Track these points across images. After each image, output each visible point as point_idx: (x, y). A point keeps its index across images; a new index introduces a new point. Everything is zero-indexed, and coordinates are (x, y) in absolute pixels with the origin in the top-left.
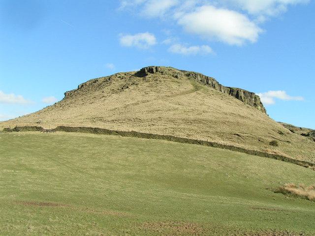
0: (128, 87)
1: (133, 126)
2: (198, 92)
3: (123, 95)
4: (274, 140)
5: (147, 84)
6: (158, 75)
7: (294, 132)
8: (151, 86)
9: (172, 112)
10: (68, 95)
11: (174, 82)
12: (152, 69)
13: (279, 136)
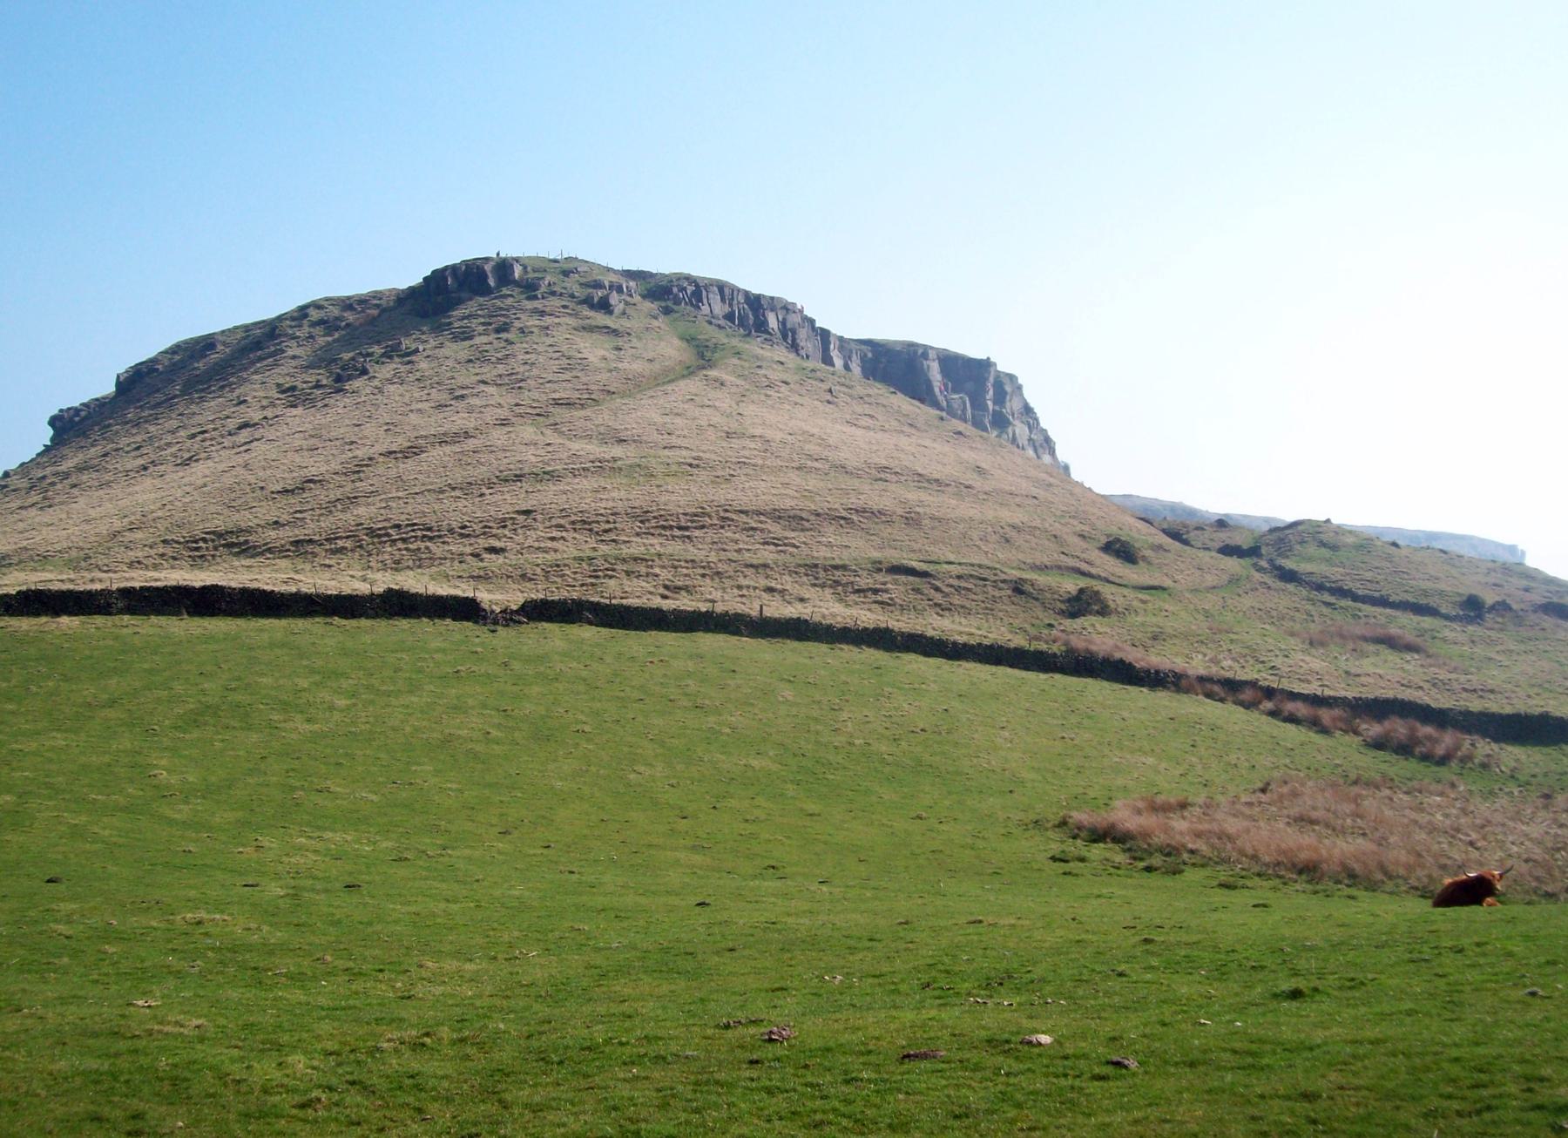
0: (364, 372)
1: (397, 566)
2: (713, 373)
3: (338, 414)
4: (1083, 583)
5: (460, 350)
6: (512, 298)
7: (1186, 543)
8: (481, 358)
9: (586, 483)
10: (71, 427)
11: (591, 329)
12: (482, 276)
13: (1110, 565)
